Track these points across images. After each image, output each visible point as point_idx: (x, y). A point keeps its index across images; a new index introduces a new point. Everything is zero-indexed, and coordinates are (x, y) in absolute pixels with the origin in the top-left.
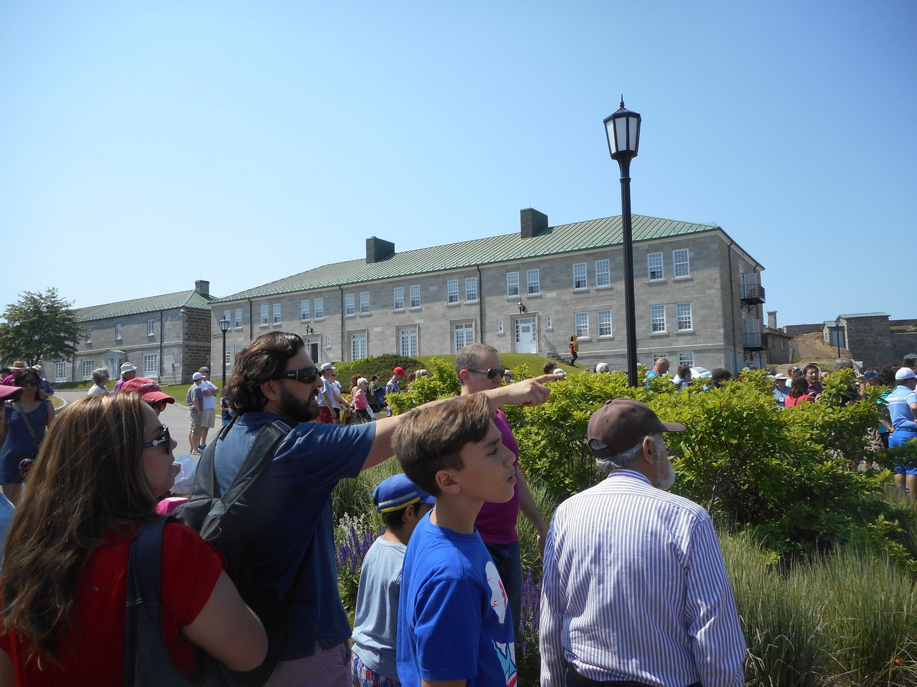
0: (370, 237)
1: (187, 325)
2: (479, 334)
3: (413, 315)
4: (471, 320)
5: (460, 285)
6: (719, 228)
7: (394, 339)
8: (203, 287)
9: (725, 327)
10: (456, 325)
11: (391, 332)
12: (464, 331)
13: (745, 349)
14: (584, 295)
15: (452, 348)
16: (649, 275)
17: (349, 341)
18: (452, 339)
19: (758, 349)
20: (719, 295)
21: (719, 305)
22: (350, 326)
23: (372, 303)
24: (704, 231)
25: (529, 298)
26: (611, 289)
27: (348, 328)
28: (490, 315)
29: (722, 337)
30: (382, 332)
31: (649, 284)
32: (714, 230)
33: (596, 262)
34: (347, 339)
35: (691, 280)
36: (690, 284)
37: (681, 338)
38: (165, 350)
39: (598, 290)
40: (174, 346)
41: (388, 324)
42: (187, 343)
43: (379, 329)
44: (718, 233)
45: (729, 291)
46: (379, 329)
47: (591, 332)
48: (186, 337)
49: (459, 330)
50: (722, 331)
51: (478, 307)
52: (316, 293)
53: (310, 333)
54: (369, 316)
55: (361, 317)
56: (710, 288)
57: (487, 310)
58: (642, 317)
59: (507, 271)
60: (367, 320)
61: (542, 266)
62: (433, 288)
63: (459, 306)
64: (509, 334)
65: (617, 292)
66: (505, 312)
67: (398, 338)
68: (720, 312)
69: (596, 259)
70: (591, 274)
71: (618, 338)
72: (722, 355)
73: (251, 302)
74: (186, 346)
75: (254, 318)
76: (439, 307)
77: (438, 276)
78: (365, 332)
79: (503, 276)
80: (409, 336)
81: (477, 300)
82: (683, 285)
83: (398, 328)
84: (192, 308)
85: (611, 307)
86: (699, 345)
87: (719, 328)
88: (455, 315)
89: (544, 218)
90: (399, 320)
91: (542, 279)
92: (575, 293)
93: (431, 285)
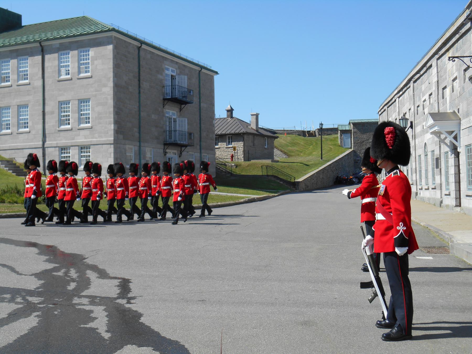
6: (113, 30)
9: (116, 122)
13: (165, 144)
19: (186, 146)
20: (111, 92)
21: (111, 102)
24: (102, 32)
29: (112, 132)
32: (109, 30)
37: (82, 132)
44: (114, 34)
50: (112, 127)
56: (105, 86)
58: (52, 113)
68: (112, 109)
71: (33, 132)
72: (111, 149)
86: (94, 140)
87: (110, 124)
89: (19, 17)
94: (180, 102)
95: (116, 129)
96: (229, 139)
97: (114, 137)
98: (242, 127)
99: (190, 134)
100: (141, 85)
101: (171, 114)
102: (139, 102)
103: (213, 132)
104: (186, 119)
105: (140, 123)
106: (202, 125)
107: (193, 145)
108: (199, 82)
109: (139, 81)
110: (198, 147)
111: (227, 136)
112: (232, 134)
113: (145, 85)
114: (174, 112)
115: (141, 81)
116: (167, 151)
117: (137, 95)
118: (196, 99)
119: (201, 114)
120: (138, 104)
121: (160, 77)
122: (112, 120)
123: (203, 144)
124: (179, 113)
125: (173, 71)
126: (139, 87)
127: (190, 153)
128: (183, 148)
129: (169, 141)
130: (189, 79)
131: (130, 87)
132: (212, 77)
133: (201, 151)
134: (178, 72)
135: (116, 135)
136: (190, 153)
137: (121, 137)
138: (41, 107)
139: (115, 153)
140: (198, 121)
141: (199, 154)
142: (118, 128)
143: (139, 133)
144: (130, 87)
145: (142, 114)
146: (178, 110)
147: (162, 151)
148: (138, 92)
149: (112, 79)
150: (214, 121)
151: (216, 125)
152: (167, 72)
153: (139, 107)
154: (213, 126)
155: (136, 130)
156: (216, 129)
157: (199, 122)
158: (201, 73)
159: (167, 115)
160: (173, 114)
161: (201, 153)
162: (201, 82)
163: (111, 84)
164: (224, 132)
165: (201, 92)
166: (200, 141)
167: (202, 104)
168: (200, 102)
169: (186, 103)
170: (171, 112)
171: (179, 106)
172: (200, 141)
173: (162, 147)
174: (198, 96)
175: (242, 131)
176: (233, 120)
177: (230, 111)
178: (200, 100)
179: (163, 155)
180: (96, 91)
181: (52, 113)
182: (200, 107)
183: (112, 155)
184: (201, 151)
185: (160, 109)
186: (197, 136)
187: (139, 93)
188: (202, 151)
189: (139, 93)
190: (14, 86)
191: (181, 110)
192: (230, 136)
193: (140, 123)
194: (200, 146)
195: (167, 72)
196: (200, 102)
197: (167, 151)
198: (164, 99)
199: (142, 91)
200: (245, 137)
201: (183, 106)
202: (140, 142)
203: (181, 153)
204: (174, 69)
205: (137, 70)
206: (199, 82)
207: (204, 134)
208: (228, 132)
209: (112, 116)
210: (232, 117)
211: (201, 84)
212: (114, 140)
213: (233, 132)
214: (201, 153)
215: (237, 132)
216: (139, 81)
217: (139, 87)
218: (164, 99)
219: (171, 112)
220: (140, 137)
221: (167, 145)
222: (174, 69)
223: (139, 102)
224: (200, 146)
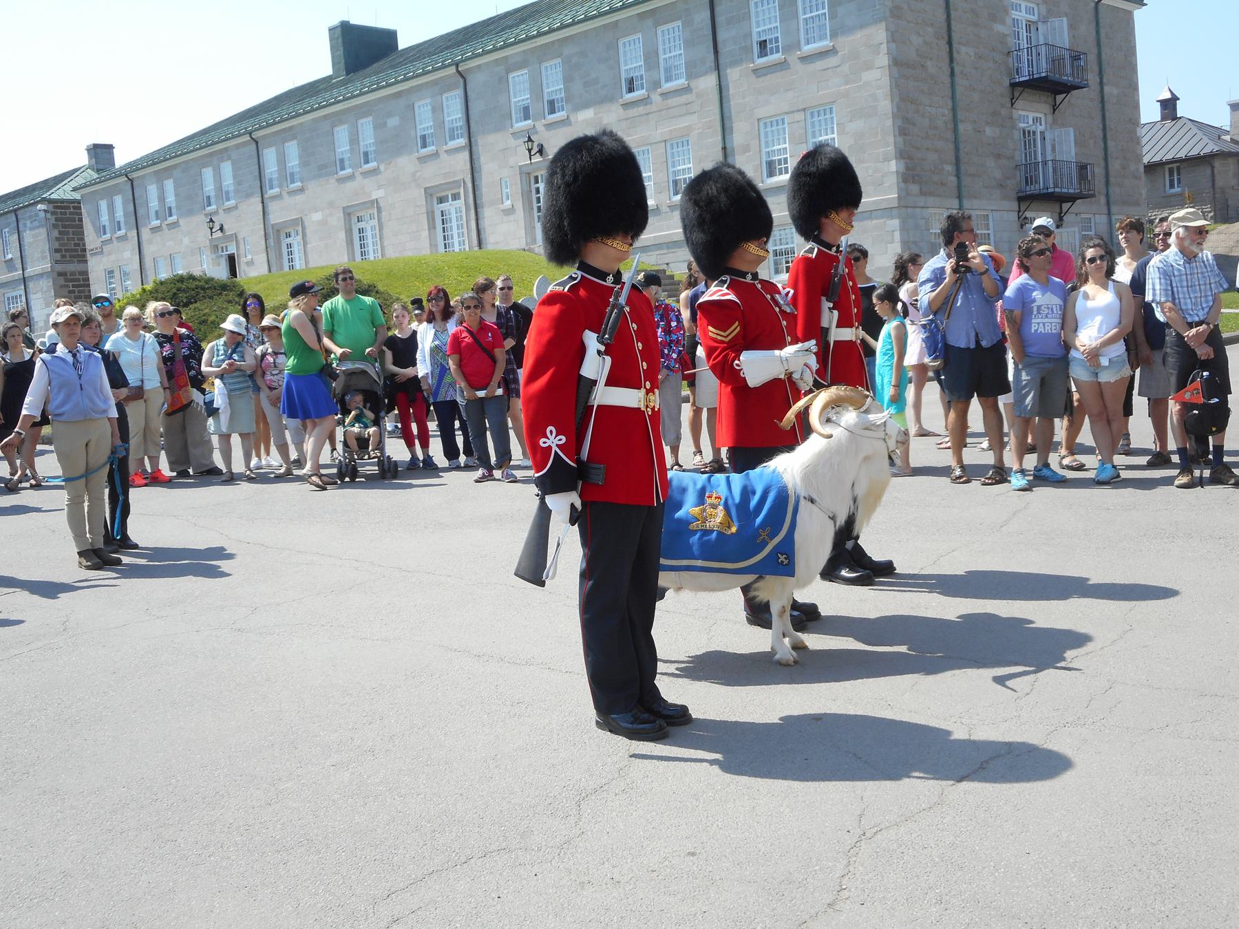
0: (335, 22)
1: (56, 233)
2: (473, 212)
3: (369, 183)
4: (456, 184)
5: (434, 110)
7: (342, 235)
8: (101, 153)
9: (902, 155)
10: (437, 196)
11: (337, 219)
12: (450, 207)
13: (1021, 199)
14: (641, 110)
15: (433, 245)
16: (756, 49)
17: (279, 242)
18: (432, 226)
19: (1072, 199)
20: (886, 81)
21: (885, 105)
22: (275, 217)
23: (304, 164)
25: (549, 126)
26: (687, 90)
27: (275, 217)
28: (488, 167)
29: (892, 181)
30: (324, 223)
31: (755, 71)
33: (660, 29)
34: (275, 237)
35: (831, 52)
36: (832, 61)
38: (31, 285)
39: (665, 95)
40: (41, 275)
41: (331, 204)
42: (59, 268)
43: (317, 216)
45: (937, 67)
46: (317, 216)
47: (659, 191)
48: (58, 256)
49: (444, 206)
50: (893, 166)
51: (466, 154)
52: (221, 151)
53: (219, 234)
54: (302, 190)
55: (292, 193)
56: (869, 66)
57: (482, 159)
58: (746, 148)
59: (509, 71)
60: (299, 198)
61: (567, 51)
62: (393, 122)
63: (436, 155)
64: (519, 206)
65: (698, 96)
66: (512, 161)
67: (349, 232)
68: (889, 123)
69: (658, 24)
70: (651, 58)
72: (895, 223)
73: (132, 181)
74: (60, 274)
75: (141, 212)
76: (406, 163)
77: (398, 95)
78: (300, 222)
79: (503, 80)
80: (369, 225)
81: (462, 141)
82: (820, 64)
83: (347, 213)
84: (62, 201)
85: (689, 128)
87: (887, 160)
88: (434, 174)
90: (347, 194)
91: (568, 80)
92: (626, 106)
93: (390, 115)
94: (1051, 88)
95: (902, 169)
96: (1171, 174)
97: (899, 190)
98: (1206, 140)
99: (1082, 168)
100: (955, 55)
101: (1031, 122)
102: (953, 98)
103: (1139, 157)
104: (1071, 130)
105: (957, 149)
106: (1110, 143)
107: (1092, 196)
108: (1098, 33)
109: (950, 43)
110: (1103, 200)
111: (1167, 167)
112: (1181, 161)
113: (965, 53)
114: (1039, 115)
115: (955, 45)
116: (1028, 214)
117: (947, 80)
118: (1092, 78)
119: (1107, 115)
120: (950, 103)
121: (999, 28)
122: (891, 148)
123: (1115, 191)
124: (1050, 118)
125: (1030, 11)
126: (951, 60)
127: (1083, 216)
128: (1065, 206)
129: (1032, 189)
130: (1071, 27)
131: (929, 63)
132: (1129, 15)
133: (1109, 210)
134: (1043, 9)
135: (903, 185)
136: (1083, 216)
137: (915, 188)
138: (720, 138)
139: (904, 229)
140: (1100, 134)
141: (1104, 218)
142: (908, 168)
143: (958, 176)
144: (929, 63)
145: (961, 127)
146: (1047, 108)
147: (1013, 216)
148: (948, 72)
149: (884, 47)
150: (1138, 130)
151: (1144, 140)
152: (1015, 14)
153: (954, 110)
154: (1137, 141)
155: (949, 168)
156: (1145, 150)
157: (1101, 135)
158: (1100, 7)
159: (1022, 125)
160: (1036, 120)
161: (1109, 214)
162: (1102, 31)
163: (883, 60)
164: (1156, 159)
165: (1104, 57)
166: (1107, 183)
167: (1107, 89)
168: (1101, 83)
169: (1067, 88)
170: (1031, 115)
171: (1050, 100)
172: (1107, 183)
173: (1015, 205)
174: (1096, 68)
175: (1207, 150)
176: (1180, 123)
177: (1169, 106)
178: (1101, 79)
179: (1016, 225)
180: (847, 83)
181: (746, 148)
182: (1102, 97)
183: (897, 235)
184: (1109, 210)
185: (1004, 112)
186: (1099, 171)
187: (952, 74)
188: (1114, 209)
189: (952, 74)
190: (656, 97)
191: (1055, 108)
192: (1174, 165)
193: (957, 149)
194: (1107, 195)
195: (1015, 14)
196: (1101, 83)
197: (1028, 214)
198: (1014, 85)
199: (957, 69)
200: (1217, 163)
201: (1060, 98)
202: (959, 197)
203: (1061, 219)
204: (1032, 5)
205: (941, 16)
206: (1098, 33)
207: (1115, 166)
208: (1169, 156)
209: (891, 139)
210: (1175, 118)
211: (1103, 36)
212: (899, 198)
213: (1182, 155)
214: (1109, 214)
215: (1194, 152)
216: (950, 43)
217: (951, 60)
218: (1014, 85)
219: (1031, 115)
220: (959, 187)
221: (1029, 199)
222: (1032, 5)
223: (953, 98)
224: (1107, 195)
